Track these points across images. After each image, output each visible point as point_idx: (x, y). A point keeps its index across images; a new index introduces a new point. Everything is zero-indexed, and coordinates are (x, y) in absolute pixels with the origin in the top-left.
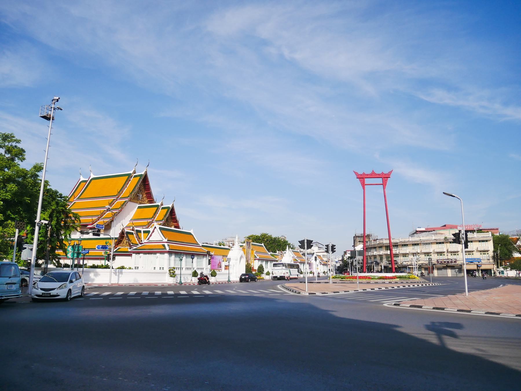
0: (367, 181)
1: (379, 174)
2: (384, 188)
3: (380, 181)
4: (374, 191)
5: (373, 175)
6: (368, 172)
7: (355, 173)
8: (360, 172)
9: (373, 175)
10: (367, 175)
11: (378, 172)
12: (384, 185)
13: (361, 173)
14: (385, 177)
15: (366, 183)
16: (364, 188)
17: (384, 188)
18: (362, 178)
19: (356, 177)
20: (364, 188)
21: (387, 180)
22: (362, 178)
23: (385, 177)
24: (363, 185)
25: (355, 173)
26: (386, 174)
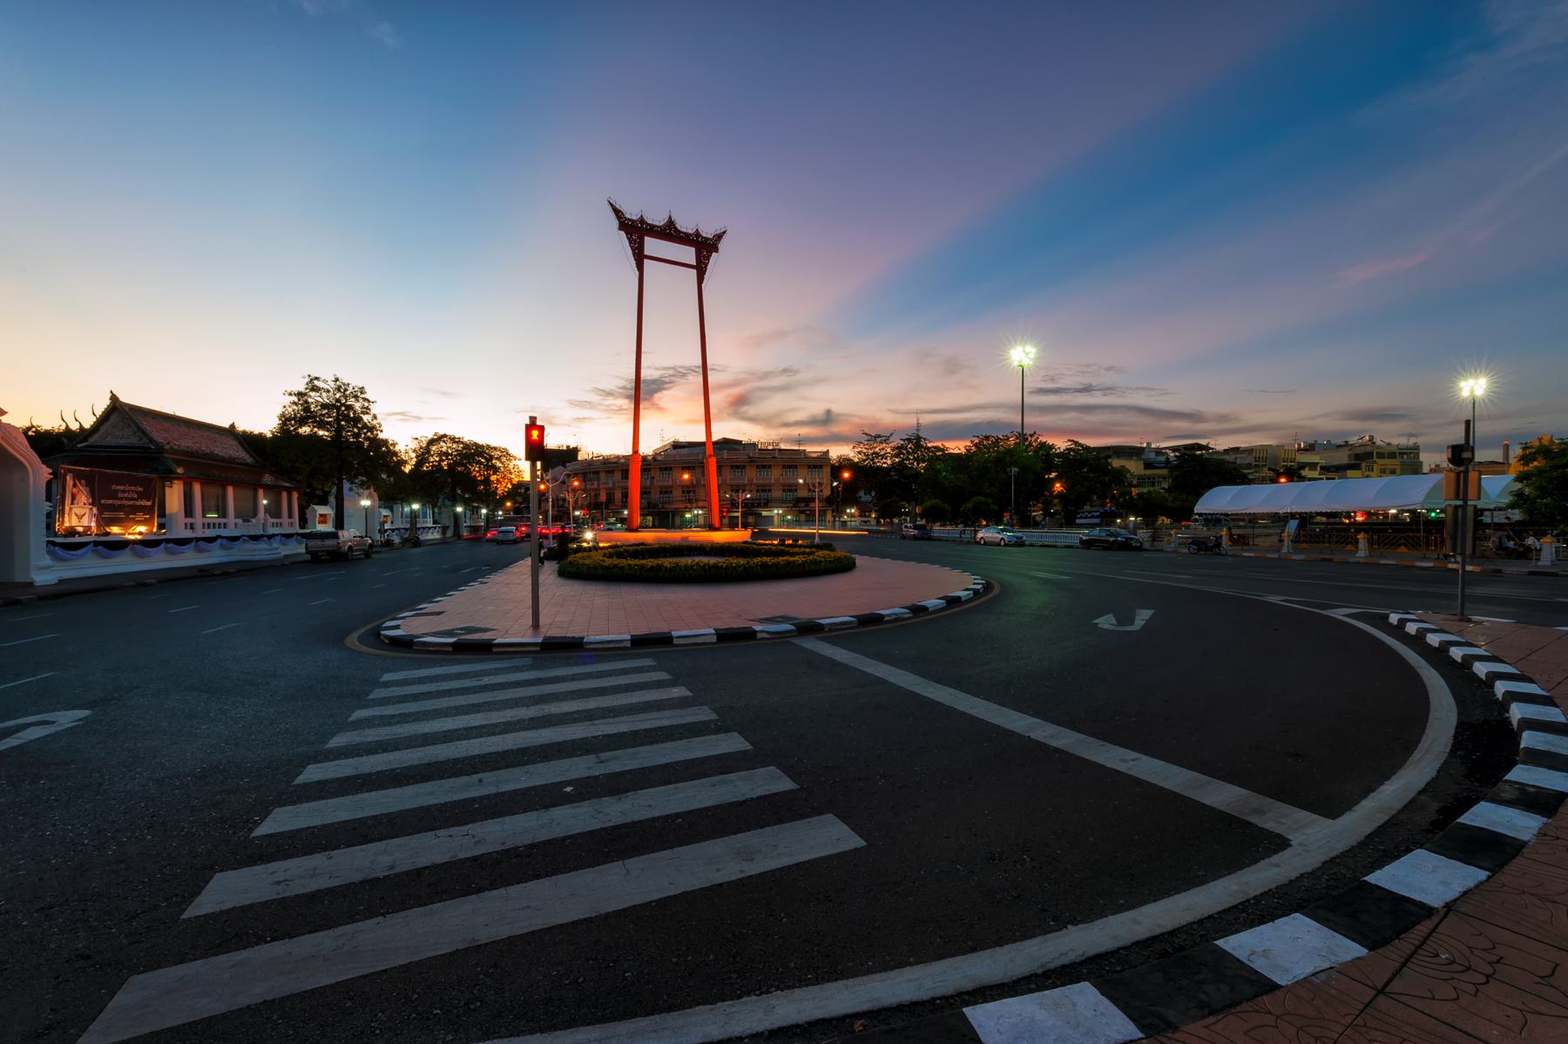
0: (652, 246)
1: (688, 235)
3: (688, 254)
4: (670, 283)
5: (669, 232)
6: (657, 219)
7: (618, 212)
8: (632, 213)
9: (669, 232)
10: (653, 226)
11: (685, 225)
14: (705, 247)
16: (640, 267)
18: (636, 231)
19: (616, 223)
20: (640, 267)
23: (705, 247)
24: (640, 257)
25: (618, 212)
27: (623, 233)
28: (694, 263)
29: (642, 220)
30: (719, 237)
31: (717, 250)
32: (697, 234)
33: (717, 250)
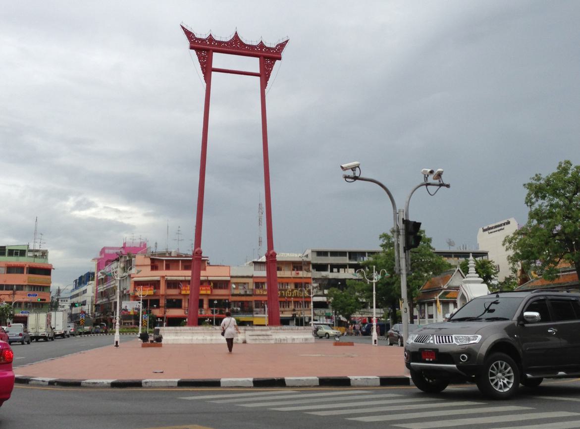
0: (219, 60)
2: (264, 85)
3: (253, 64)
5: (236, 47)
6: (224, 36)
7: (189, 34)
9: (236, 47)
10: (220, 43)
11: (249, 38)
12: (264, 75)
13: (204, 37)
15: (214, 66)
16: (208, 79)
17: (264, 85)
18: (205, 49)
19: (187, 43)
20: (208, 79)
21: (272, 66)
22: (205, 49)
23: (268, 56)
24: (207, 69)
25: (189, 34)
26: (269, 49)
27: (193, 52)
28: (258, 71)
29: (211, 39)
30: (282, 46)
31: (280, 59)
32: (262, 45)
33: (280, 59)
